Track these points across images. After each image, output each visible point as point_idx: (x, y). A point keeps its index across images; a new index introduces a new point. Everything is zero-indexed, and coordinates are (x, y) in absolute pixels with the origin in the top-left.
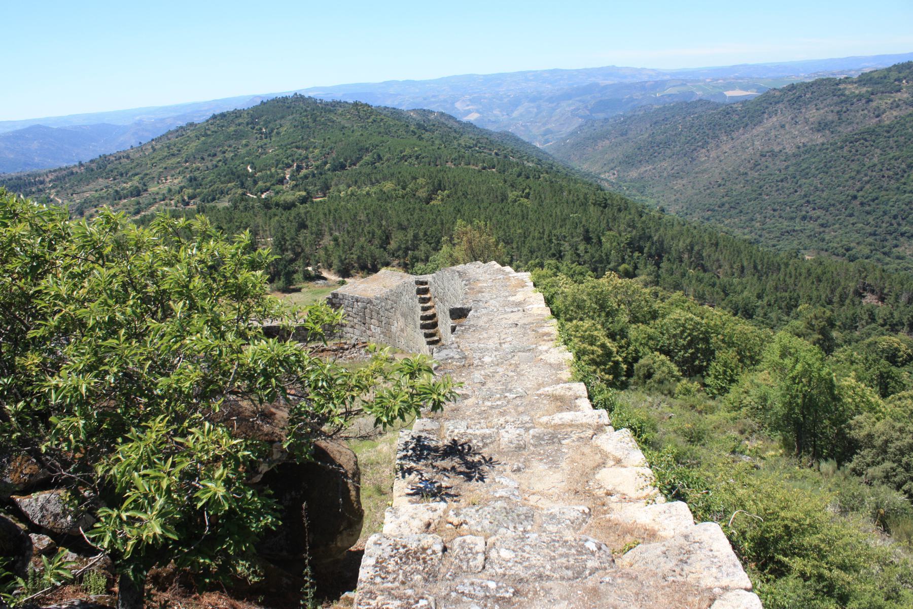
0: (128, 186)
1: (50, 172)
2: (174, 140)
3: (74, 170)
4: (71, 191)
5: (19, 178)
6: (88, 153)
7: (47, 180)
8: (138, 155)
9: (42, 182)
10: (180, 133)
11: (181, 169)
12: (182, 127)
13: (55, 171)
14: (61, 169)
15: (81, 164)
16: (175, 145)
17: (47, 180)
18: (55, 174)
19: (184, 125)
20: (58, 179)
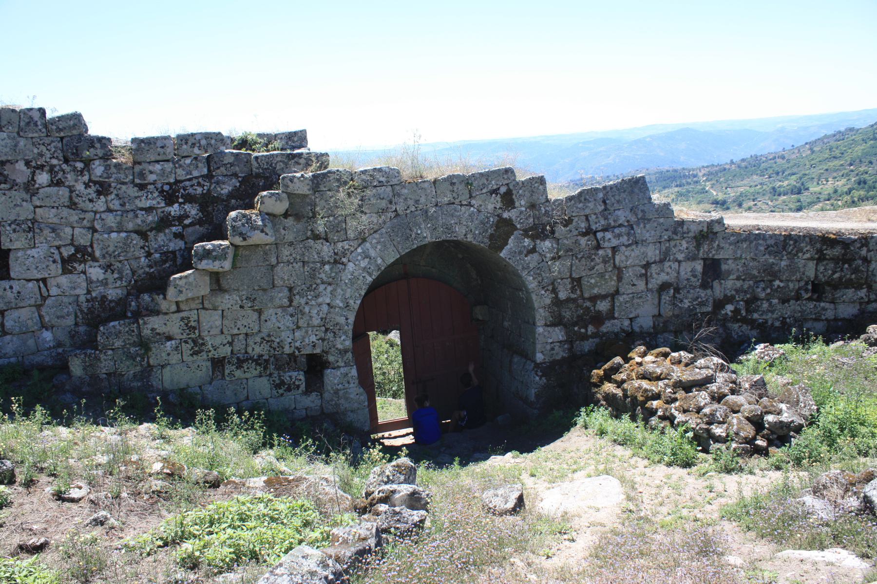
0: (786, 183)
1: (703, 167)
2: (833, 143)
3: (727, 167)
4: (726, 185)
5: (676, 171)
6: (740, 153)
7: (700, 174)
8: (794, 156)
9: (695, 176)
10: (837, 137)
11: (846, 171)
12: (840, 132)
13: (707, 167)
14: (713, 165)
15: (732, 162)
16: (837, 148)
17: (700, 174)
18: (707, 170)
19: (842, 129)
20: (710, 174)
